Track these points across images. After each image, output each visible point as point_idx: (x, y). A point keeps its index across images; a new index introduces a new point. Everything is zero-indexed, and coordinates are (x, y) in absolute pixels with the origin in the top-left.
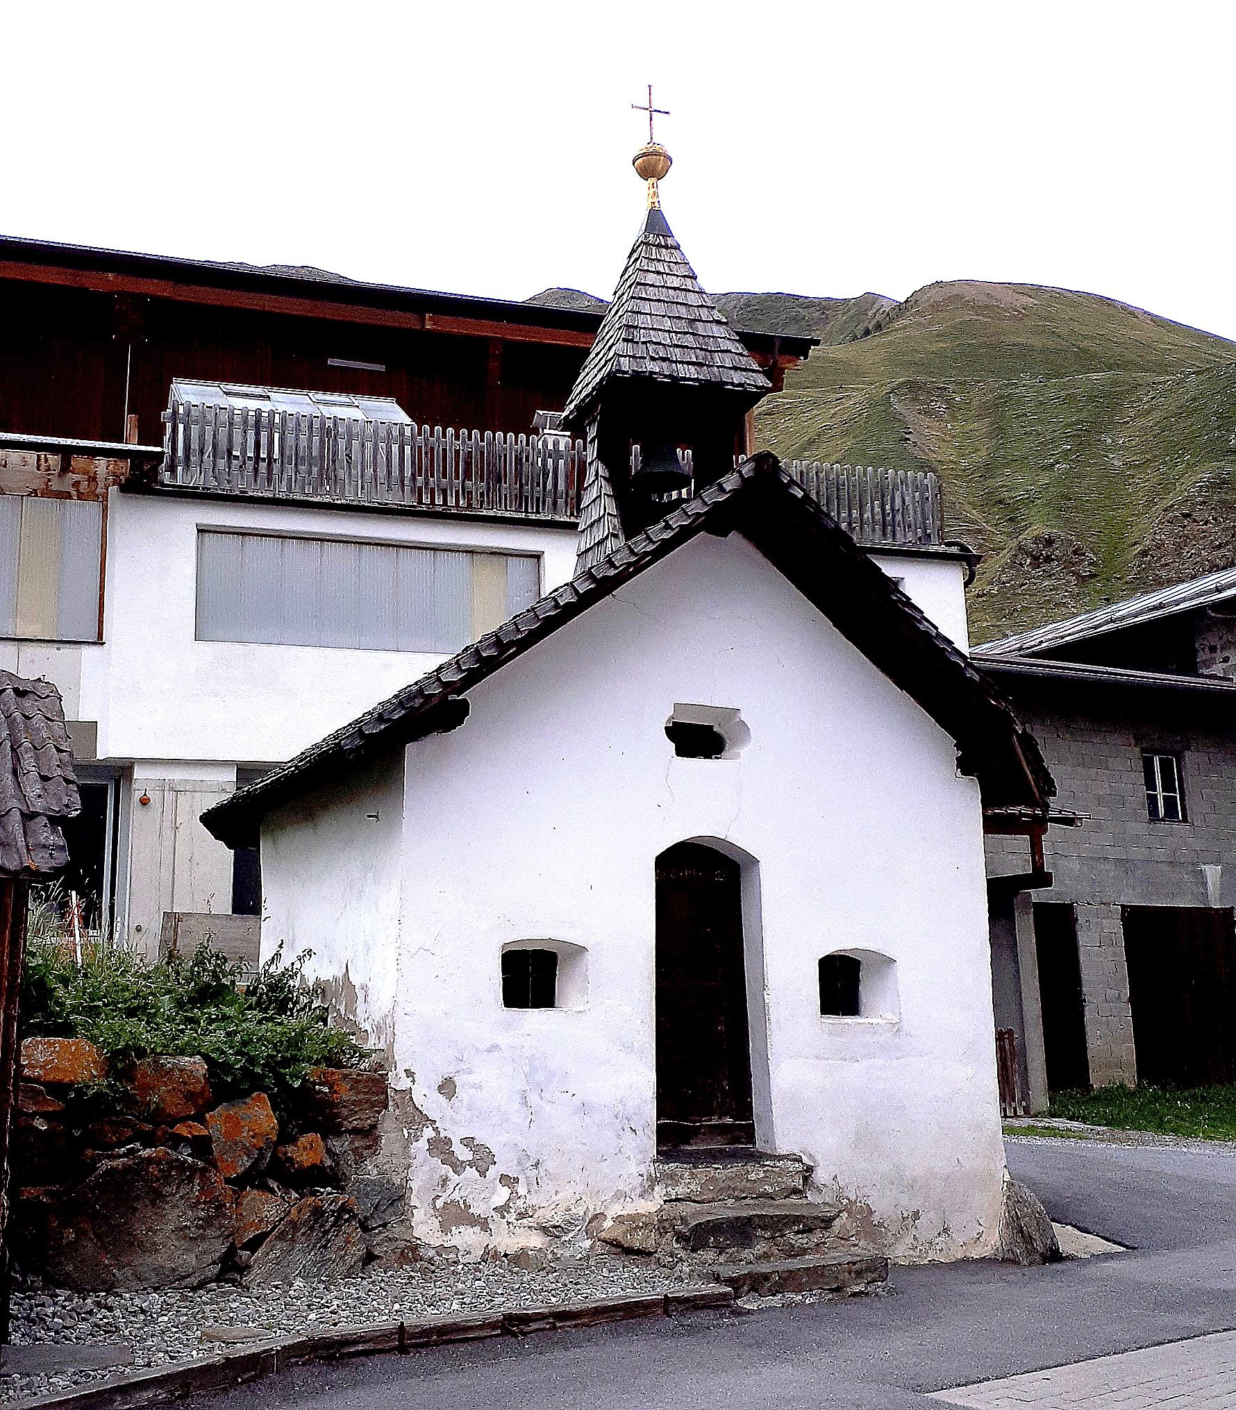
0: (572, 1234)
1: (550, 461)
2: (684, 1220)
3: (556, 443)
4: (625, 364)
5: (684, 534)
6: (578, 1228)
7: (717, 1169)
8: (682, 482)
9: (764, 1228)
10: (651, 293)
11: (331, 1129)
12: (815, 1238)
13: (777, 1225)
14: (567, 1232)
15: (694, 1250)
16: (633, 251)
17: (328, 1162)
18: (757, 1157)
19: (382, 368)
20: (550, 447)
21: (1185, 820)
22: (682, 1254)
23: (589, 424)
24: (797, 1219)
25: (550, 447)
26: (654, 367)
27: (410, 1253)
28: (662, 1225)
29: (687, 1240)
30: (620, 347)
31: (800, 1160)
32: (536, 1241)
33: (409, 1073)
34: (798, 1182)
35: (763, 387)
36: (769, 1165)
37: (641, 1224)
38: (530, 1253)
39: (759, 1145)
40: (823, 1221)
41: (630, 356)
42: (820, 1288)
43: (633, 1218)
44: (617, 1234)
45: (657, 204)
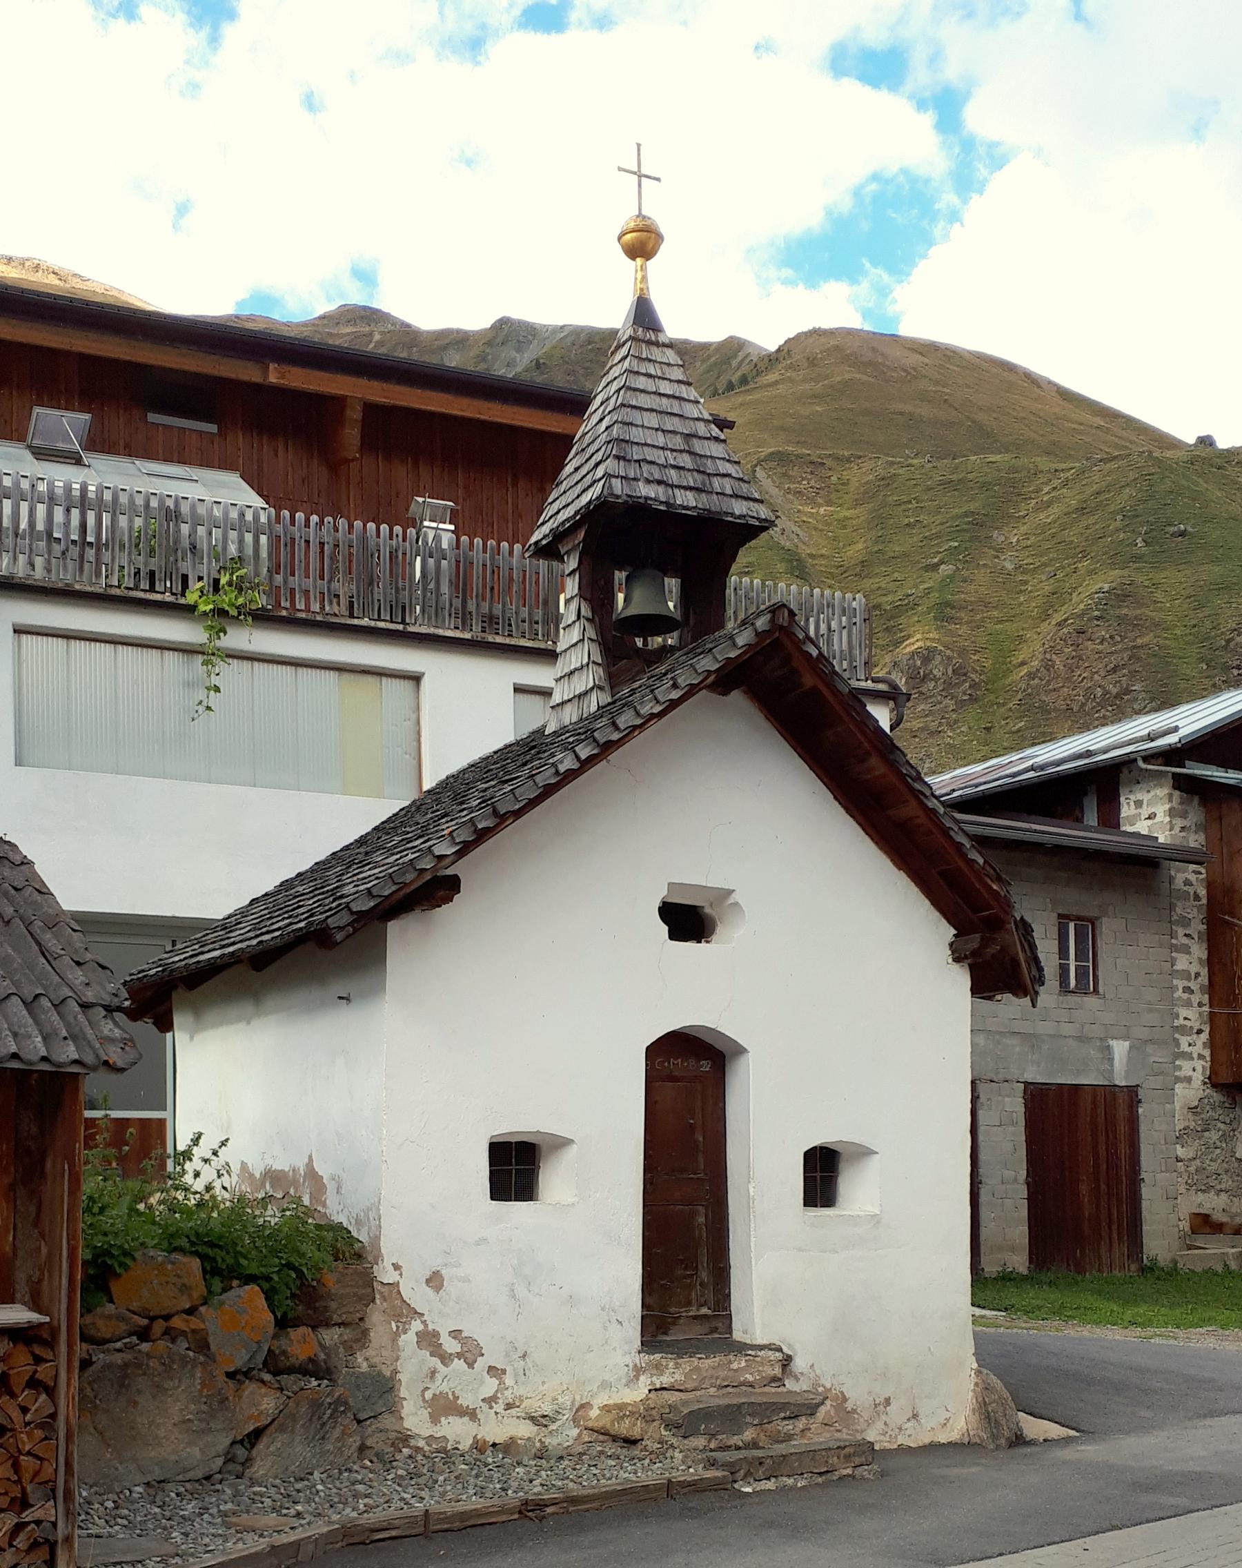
0: (559, 1423)
3: (437, 538)
4: (617, 485)
5: (692, 690)
6: (565, 1417)
7: (700, 1359)
10: (643, 401)
12: (801, 1423)
14: (554, 1420)
15: (685, 1437)
17: (322, 1356)
21: (1096, 991)
22: (674, 1441)
23: (568, 553)
24: (784, 1407)
26: (645, 490)
28: (646, 1414)
30: (611, 465)
31: (780, 1350)
32: (525, 1430)
33: (396, 1267)
34: (777, 1371)
35: (766, 520)
38: (519, 1442)
39: (738, 1335)
41: (622, 477)
43: (621, 1407)
44: (605, 1422)
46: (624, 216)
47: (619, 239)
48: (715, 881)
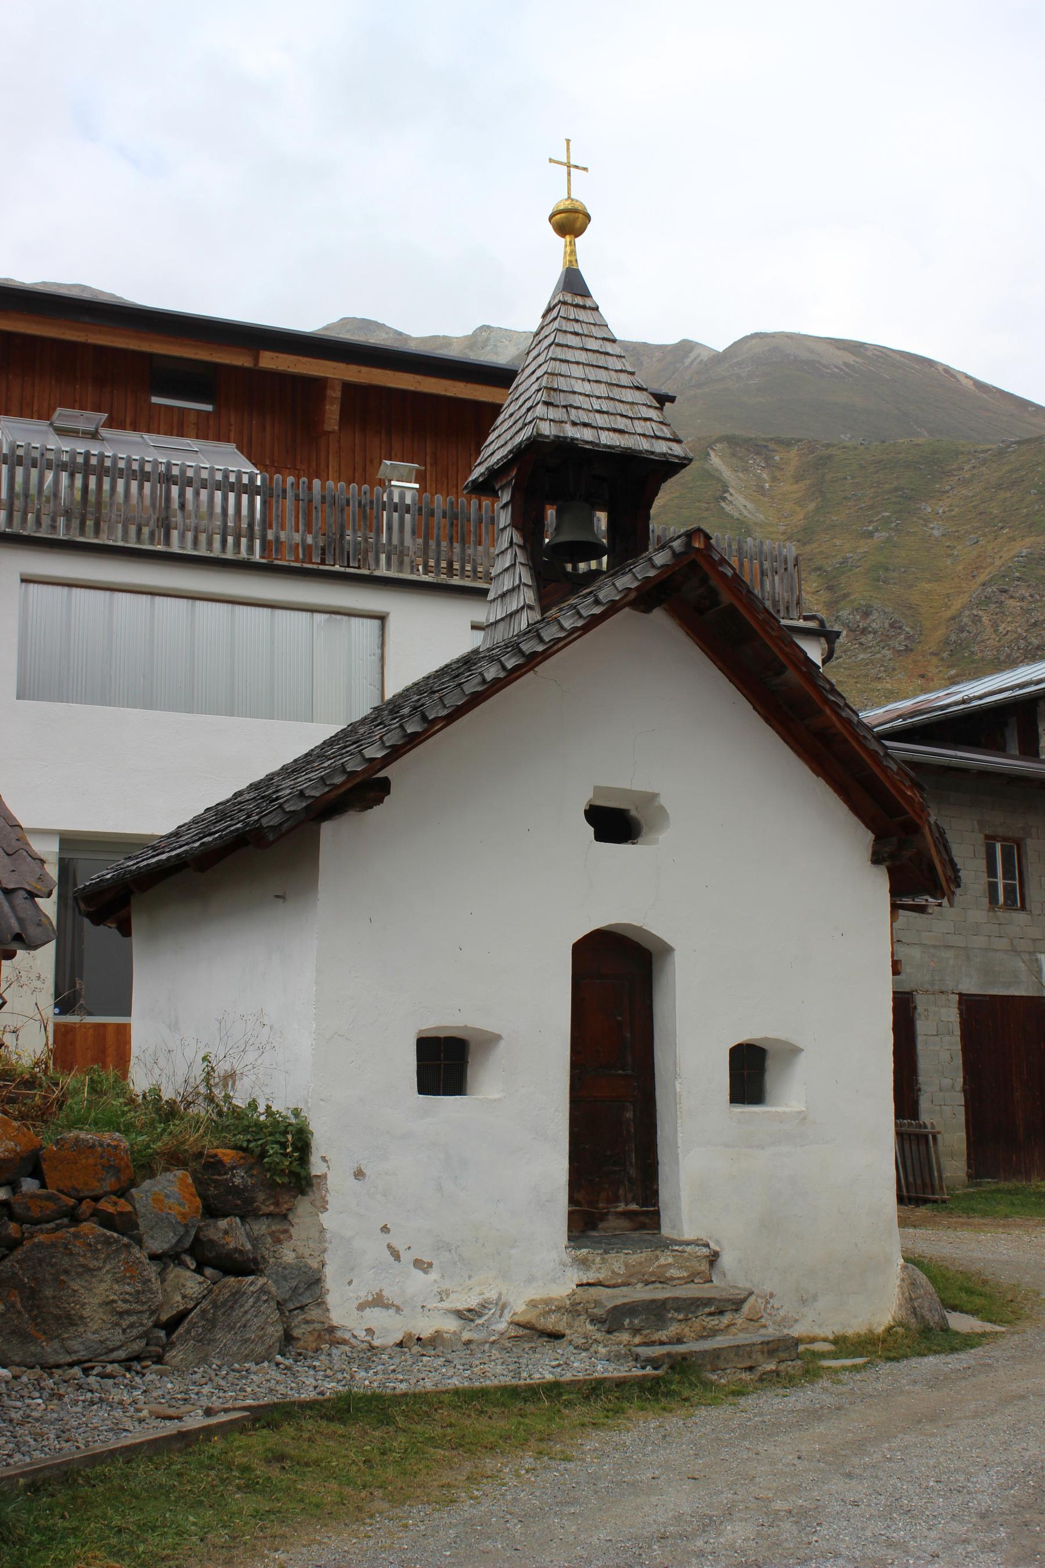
0: (486, 1318)
1: (396, 515)
2: (597, 1303)
4: (547, 429)
5: (613, 608)
6: (492, 1312)
7: (626, 1254)
8: (592, 551)
9: (678, 1310)
10: (569, 355)
11: (247, 1213)
12: (726, 1319)
13: (691, 1306)
14: (480, 1315)
15: (609, 1332)
16: (549, 310)
17: (249, 1247)
18: (666, 1244)
19: (209, 408)
20: (396, 500)
22: (598, 1336)
23: (502, 488)
24: (709, 1301)
25: (396, 500)
26: (570, 432)
27: (329, 1334)
28: (573, 1309)
29: (602, 1322)
30: (540, 410)
31: (707, 1245)
32: (450, 1325)
33: (324, 1159)
34: (704, 1266)
35: (685, 458)
36: (677, 1251)
37: (553, 1308)
38: (445, 1335)
39: (666, 1231)
40: (733, 1303)
41: (551, 420)
42: (735, 1368)
43: (547, 1302)
44: (531, 1317)
45: (574, 263)
46: (555, 199)
47: (550, 219)
48: (640, 785)
